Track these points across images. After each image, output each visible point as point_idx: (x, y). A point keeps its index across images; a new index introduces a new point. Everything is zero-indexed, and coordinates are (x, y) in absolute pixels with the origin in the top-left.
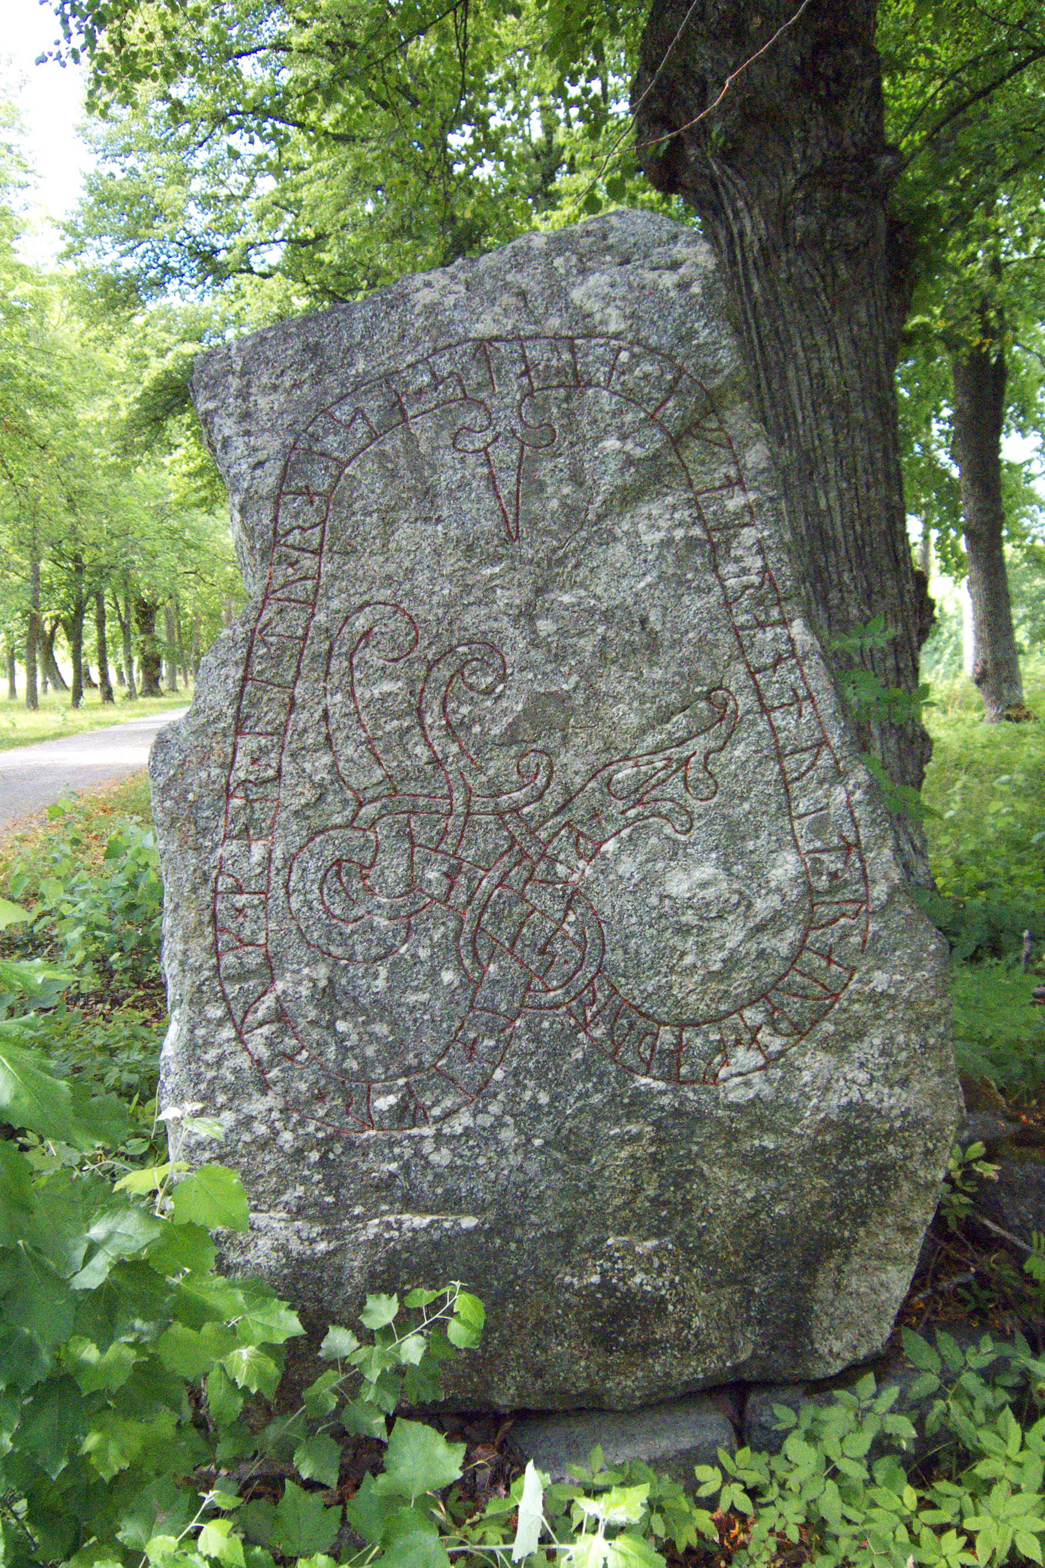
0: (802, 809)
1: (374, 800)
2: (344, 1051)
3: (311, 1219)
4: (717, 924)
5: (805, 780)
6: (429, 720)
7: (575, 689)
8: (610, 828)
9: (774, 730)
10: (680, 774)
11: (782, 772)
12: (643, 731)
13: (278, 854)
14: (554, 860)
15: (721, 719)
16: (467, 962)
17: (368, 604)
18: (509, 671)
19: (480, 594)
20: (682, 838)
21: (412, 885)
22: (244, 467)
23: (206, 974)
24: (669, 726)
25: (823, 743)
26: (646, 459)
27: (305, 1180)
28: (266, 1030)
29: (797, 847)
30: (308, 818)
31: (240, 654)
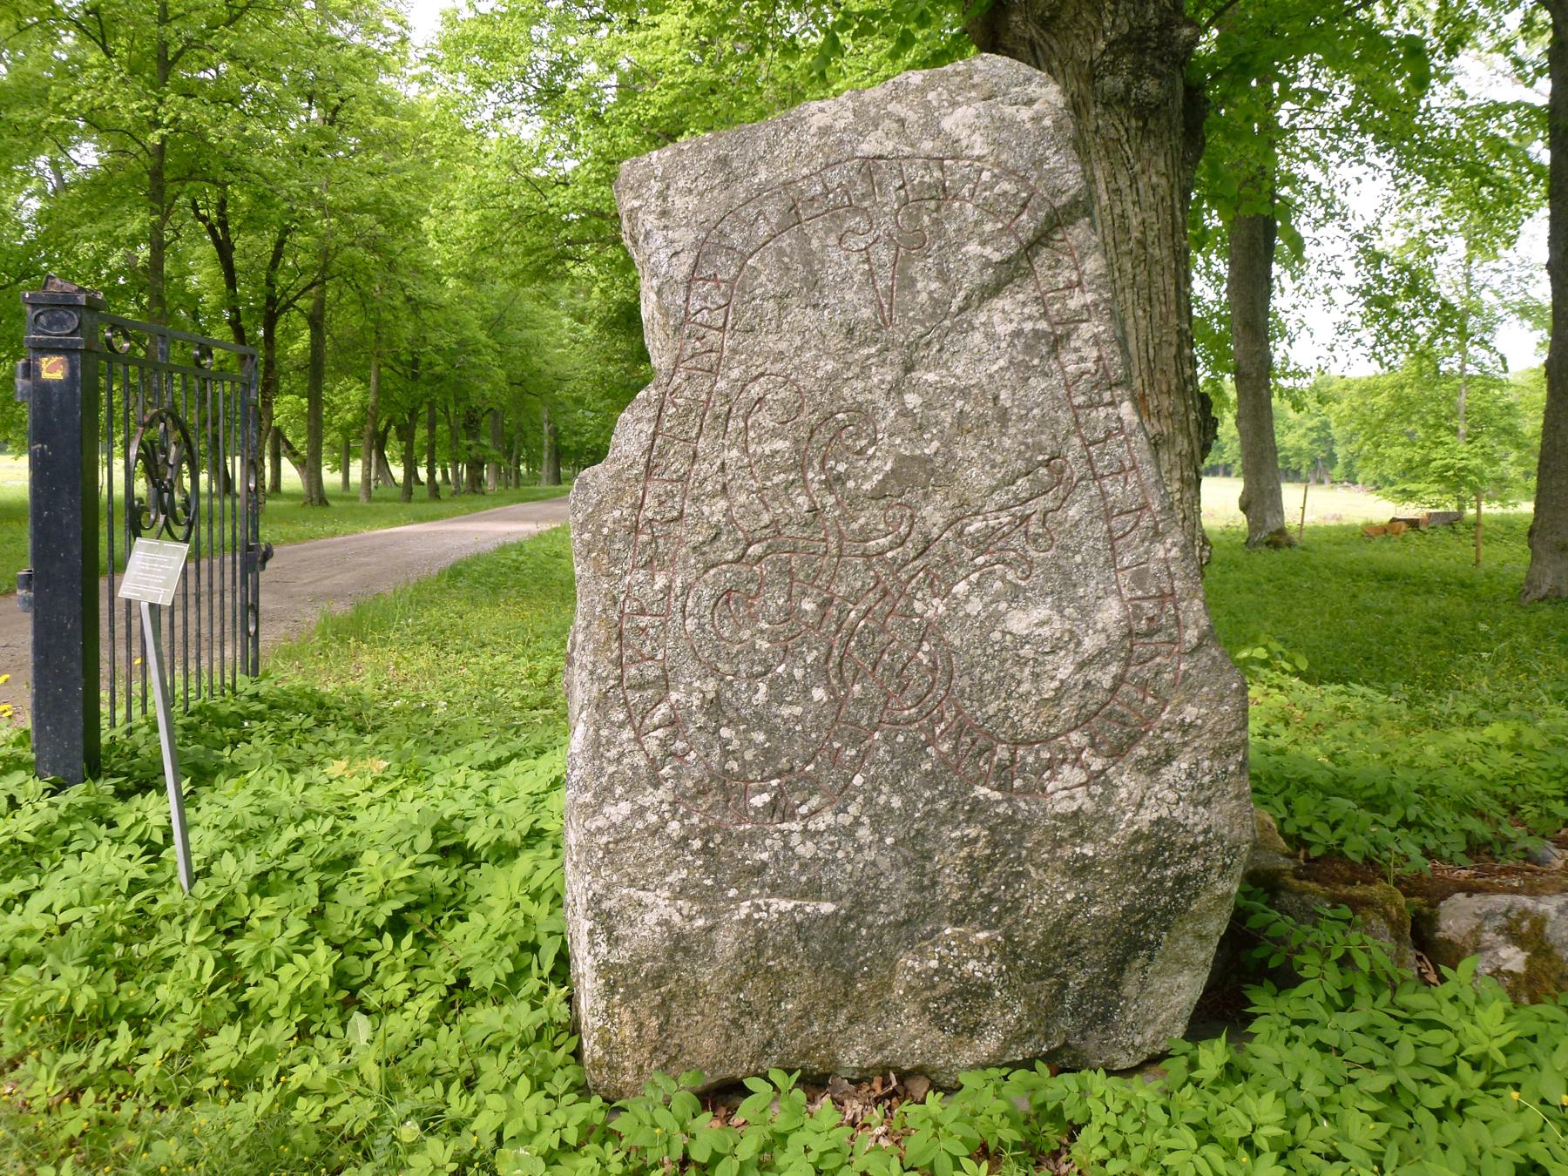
0: (1126, 563)
2: (726, 754)
3: (692, 898)
4: (1050, 658)
5: (1129, 538)
6: (810, 475)
8: (962, 572)
9: (1104, 495)
10: (1022, 528)
11: (1110, 530)
12: (993, 490)
13: (678, 583)
14: (912, 597)
15: (1059, 483)
16: (835, 682)
17: (762, 374)
18: (880, 436)
19: (857, 370)
20: (1023, 583)
21: (791, 613)
22: (662, 256)
23: (612, 682)
25: (1144, 507)
26: (1002, 262)
27: (687, 865)
28: (660, 733)
29: (1120, 594)
30: (704, 554)
31: (652, 413)
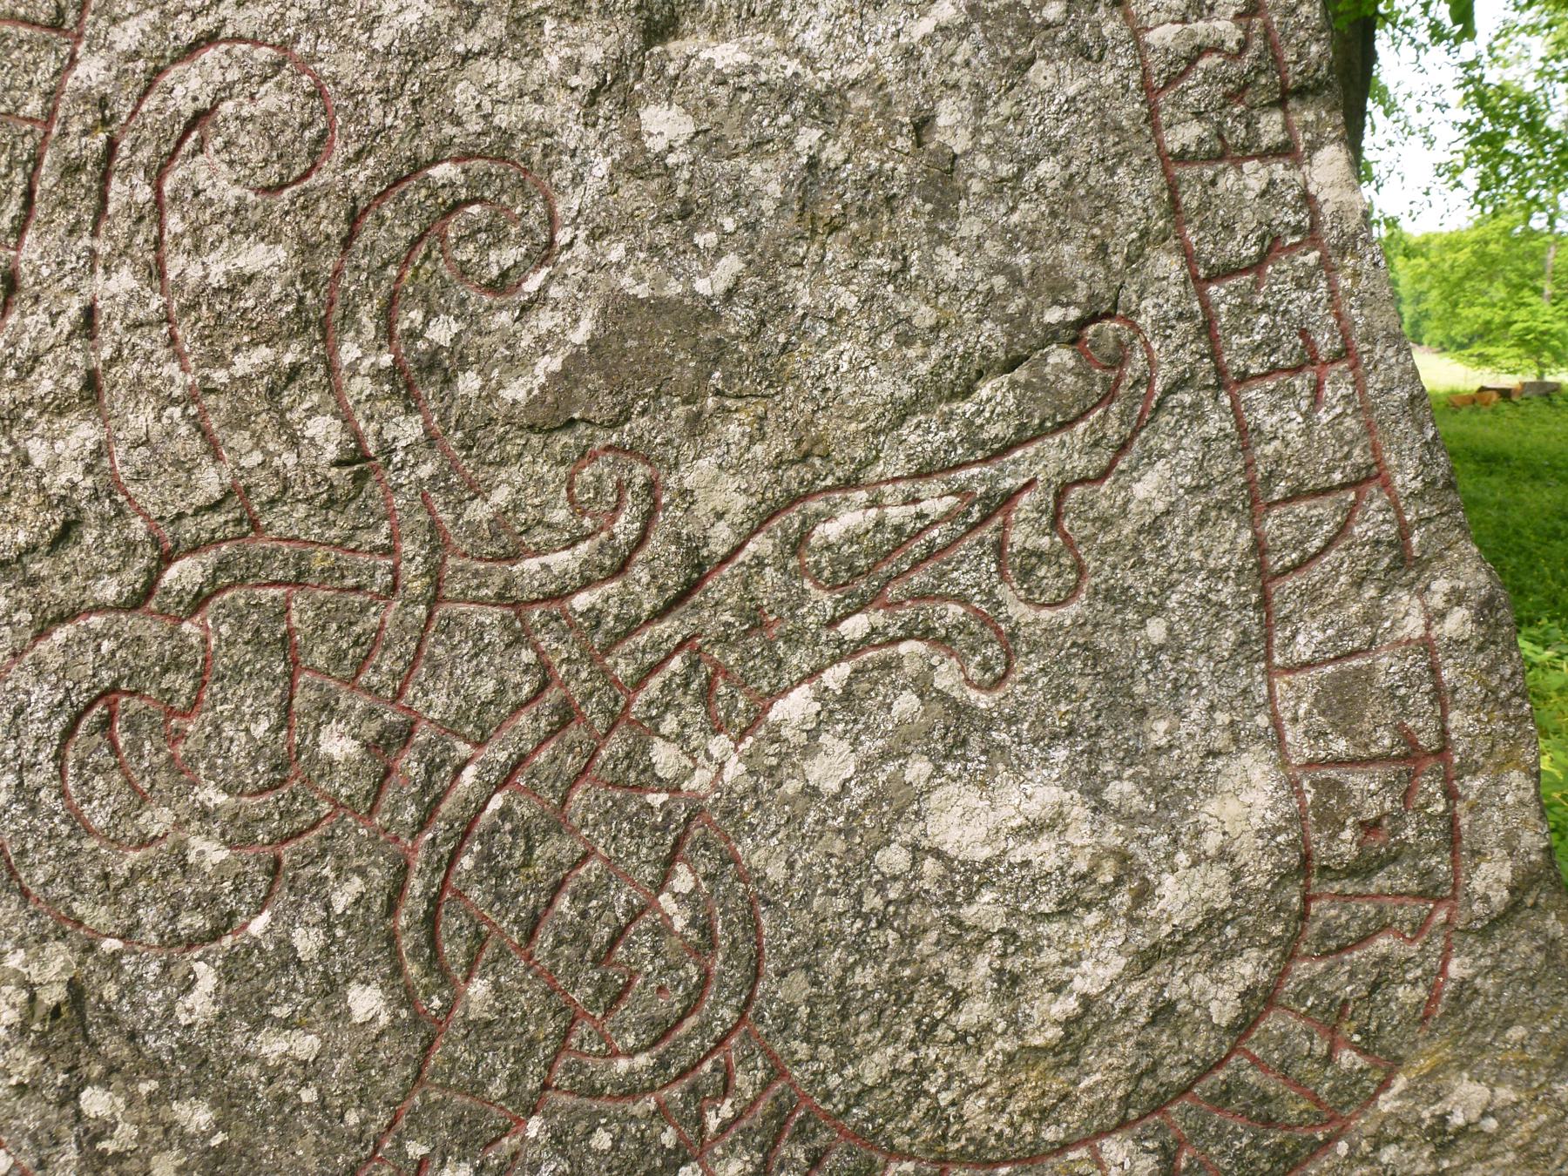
0: (1303, 648)
1: (196, 548)
4: (1053, 929)
5: (1317, 572)
6: (349, 352)
7: (729, 294)
8: (799, 659)
9: (1245, 435)
10: (988, 533)
11: (1259, 547)
12: (903, 412)
14: (647, 730)
15: (1109, 396)
16: (413, 969)
17: (211, 38)
18: (563, 237)
19: (498, 28)
20: (983, 701)
21: (287, 766)
24: (968, 407)
25: (1371, 476)
29: (1279, 742)
30: (33, 581)
